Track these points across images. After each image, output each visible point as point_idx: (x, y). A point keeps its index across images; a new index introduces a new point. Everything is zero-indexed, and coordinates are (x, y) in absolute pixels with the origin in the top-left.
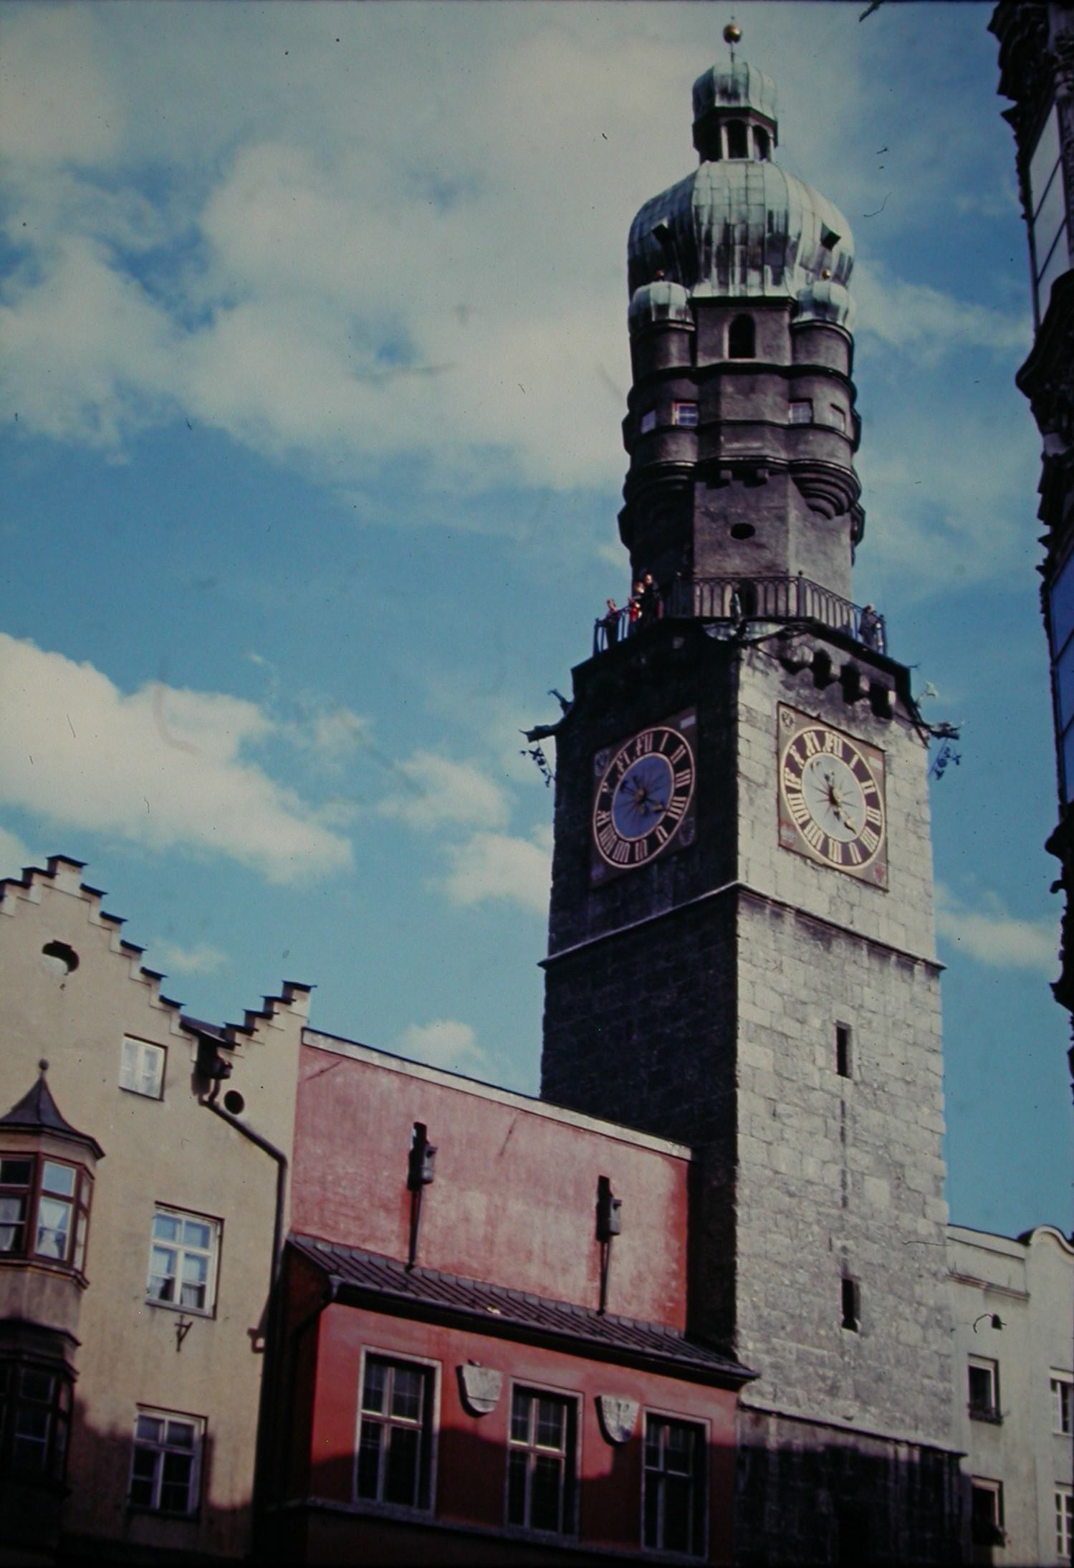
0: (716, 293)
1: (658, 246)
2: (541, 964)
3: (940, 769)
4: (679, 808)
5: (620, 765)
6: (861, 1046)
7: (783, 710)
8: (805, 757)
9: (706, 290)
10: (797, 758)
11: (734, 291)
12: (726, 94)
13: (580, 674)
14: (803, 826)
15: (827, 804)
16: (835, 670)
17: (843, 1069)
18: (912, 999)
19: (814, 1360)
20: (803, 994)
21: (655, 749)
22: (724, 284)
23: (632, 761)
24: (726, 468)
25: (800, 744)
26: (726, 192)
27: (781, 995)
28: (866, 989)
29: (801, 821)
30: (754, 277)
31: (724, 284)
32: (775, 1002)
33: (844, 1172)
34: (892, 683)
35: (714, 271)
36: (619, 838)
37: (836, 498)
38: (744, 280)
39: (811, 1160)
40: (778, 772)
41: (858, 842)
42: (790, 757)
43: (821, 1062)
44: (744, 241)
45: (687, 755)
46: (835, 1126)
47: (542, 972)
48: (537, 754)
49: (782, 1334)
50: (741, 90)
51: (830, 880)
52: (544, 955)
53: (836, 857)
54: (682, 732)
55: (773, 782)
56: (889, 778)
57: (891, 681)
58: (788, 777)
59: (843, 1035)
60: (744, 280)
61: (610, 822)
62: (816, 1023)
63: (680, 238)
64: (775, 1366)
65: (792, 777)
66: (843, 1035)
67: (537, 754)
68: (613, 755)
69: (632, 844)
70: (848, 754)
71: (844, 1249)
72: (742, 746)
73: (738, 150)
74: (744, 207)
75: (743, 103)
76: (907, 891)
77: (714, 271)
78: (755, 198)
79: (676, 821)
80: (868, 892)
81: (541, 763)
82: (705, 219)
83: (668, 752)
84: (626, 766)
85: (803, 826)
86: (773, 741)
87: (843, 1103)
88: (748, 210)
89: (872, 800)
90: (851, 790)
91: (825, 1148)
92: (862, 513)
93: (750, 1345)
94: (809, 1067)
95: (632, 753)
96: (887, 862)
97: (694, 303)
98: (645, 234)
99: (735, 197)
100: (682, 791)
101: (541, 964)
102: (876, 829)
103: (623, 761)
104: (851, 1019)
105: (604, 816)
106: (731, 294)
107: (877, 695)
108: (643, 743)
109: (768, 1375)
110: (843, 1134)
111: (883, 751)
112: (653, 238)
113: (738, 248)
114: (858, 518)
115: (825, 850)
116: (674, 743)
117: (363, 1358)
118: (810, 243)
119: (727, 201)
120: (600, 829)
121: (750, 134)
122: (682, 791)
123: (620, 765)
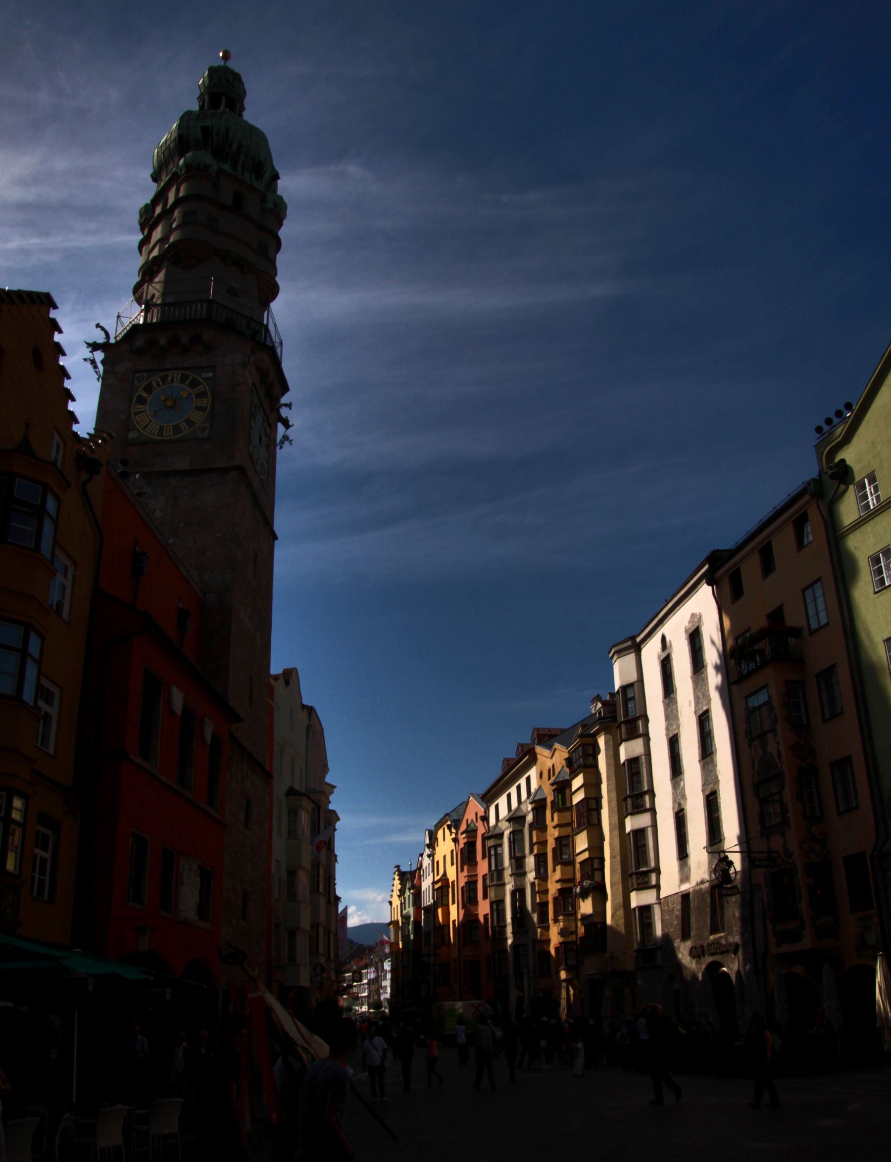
9: (227, 168)
23: (164, 384)
36: (151, 421)
48: (93, 362)
54: (203, 379)
61: (145, 411)
67: (93, 362)
79: (195, 423)
84: (158, 385)
95: (164, 379)
100: (203, 409)
103: (158, 382)
105: (140, 406)
108: (173, 377)
120: (136, 414)
122: (203, 409)
123: (155, 384)
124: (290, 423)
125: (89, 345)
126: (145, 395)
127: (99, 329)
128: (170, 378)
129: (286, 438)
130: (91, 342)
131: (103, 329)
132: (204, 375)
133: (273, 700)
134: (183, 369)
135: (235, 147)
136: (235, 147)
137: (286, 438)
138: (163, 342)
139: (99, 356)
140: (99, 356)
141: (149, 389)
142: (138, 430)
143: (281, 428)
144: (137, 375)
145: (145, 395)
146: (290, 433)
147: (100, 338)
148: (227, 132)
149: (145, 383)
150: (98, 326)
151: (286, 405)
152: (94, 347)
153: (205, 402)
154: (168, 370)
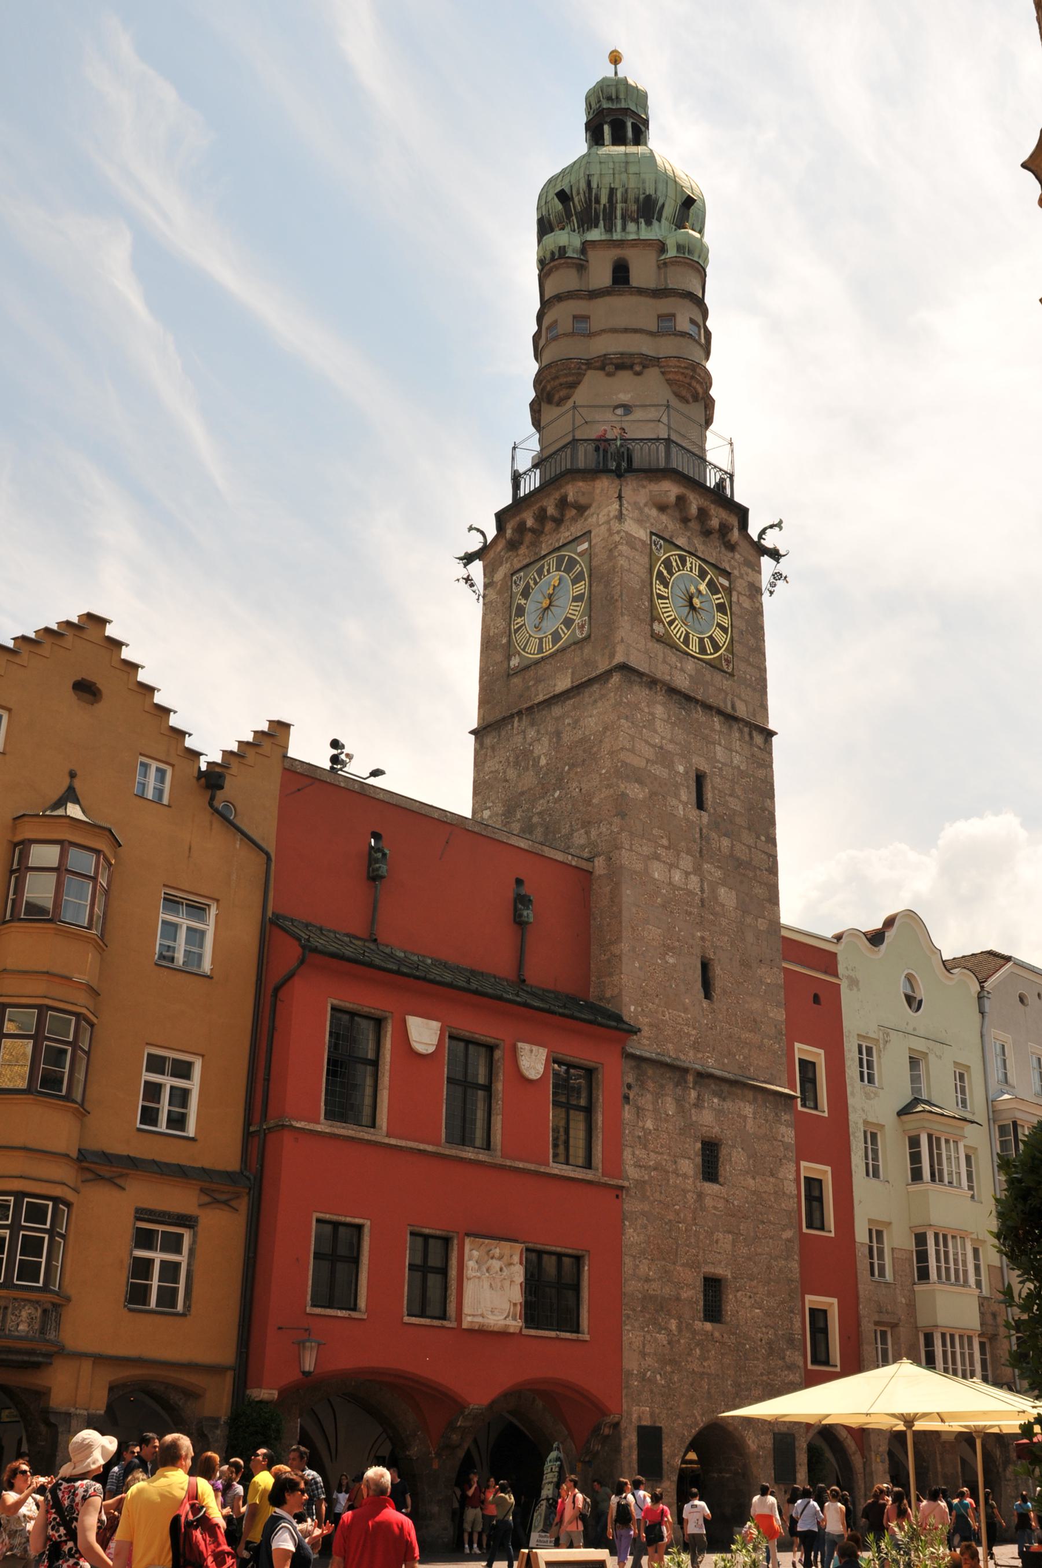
0: (604, 237)
1: (560, 206)
2: (471, 732)
3: (772, 589)
4: (576, 612)
5: (531, 582)
6: (714, 788)
7: (654, 537)
8: (671, 574)
10: (665, 573)
11: (617, 236)
12: (609, 99)
13: (501, 517)
14: (671, 623)
15: (687, 609)
16: (694, 510)
17: (700, 805)
18: (753, 755)
19: (681, 1021)
20: (670, 747)
21: (558, 569)
22: (609, 229)
23: (541, 579)
24: (612, 364)
25: (667, 564)
26: (611, 165)
27: (654, 746)
28: (718, 748)
29: (668, 619)
30: (631, 227)
31: (609, 229)
32: (649, 752)
33: (702, 881)
34: (736, 524)
35: (602, 222)
36: (530, 636)
37: (694, 388)
38: (624, 228)
39: (678, 871)
40: (651, 583)
41: (711, 638)
42: (660, 573)
43: (684, 798)
44: (625, 201)
45: (582, 572)
46: (696, 848)
47: (473, 737)
49: (657, 1001)
50: (622, 96)
51: (690, 666)
52: (474, 725)
53: (694, 648)
55: (646, 590)
56: (734, 593)
57: (734, 521)
58: (659, 588)
59: (700, 779)
60: (624, 228)
62: (681, 769)
63: (576, 199)
64: (651, 1025)
65: (661, 587)
66: (700, 779)
68: (526, 576)
69: (541, 639)
70: (702, 574)
71: (702, 938)
72: (622, 562)
73: (619, 139)
74: (624, 176)
75: (623, 105)
76: (748, 677)
77: (602, 222)
78: (632, 169)
80: (718, 677)
81: (472, 585)
82: (594, 185)
83: (568, 571)
84: (536, 583)
85: (671, 623)
86: (647, 560)
87: (701, 830)
88: (628, 178)
89: (721, 608)
90: (708, 600)
91: (687, 862)
92: (713, 401)
93: (632, 1008)
94: (674, 802)
95: (540, 572)
96: (733, 653)
97: (585, 246)
98: (549, 198)
99: (618, 168)
101: (471, 732)
102: (724, 630)
103: (535, 579)
104: (704, 766)
105: (519, 620)
106: (615, 238)
107: (724, 530)
108: (549, 565)
109: (646, 1031)
110: (701, 852)
111: (730, 574)
112: (556, 200)
113: (619, 206)
114: (709, 404)
115: (686, 641)
116: (572, 563)
117: (329, 1009)
118: (673, 202)
119: (611, 171)
120: (516, 631)
121: (629, 125)
122: (577, 599)
123: (531, 582)
124: (782, 552)
125: (461, 559)
126: (523, 602)
127: (474, 532)
128: (546, 568)
129: (777, 576)
130: (462, 555)
131: (478, 530)
132: (580, 549)
133: (836, 975)
134: (559, 549)
135: (604, 200)
136: (604, 200)
137: (777, 576)
138: (530, 523)
139: (477, 568)
140: (477, 568)
141: (526, 594)
142: (519, 653)
143: (766, 563)
144: (514, 578)
145: (523, 602)
146: (783, 566)
147: (475, 543)
148: (589, 183)
149: (522, 585)
150: (471, 529)
151: (771, 527)
152: (468, 559)
153: (581, 587)
154: (544, 557)
